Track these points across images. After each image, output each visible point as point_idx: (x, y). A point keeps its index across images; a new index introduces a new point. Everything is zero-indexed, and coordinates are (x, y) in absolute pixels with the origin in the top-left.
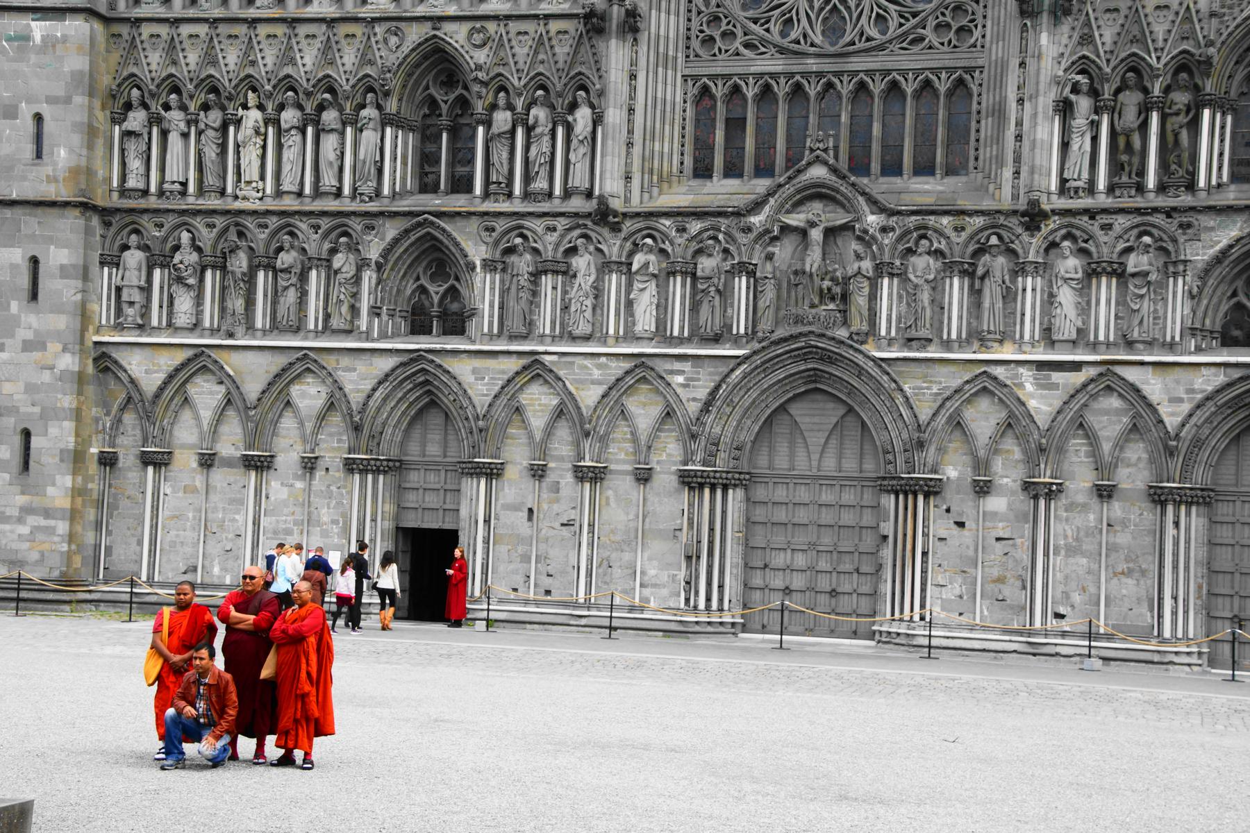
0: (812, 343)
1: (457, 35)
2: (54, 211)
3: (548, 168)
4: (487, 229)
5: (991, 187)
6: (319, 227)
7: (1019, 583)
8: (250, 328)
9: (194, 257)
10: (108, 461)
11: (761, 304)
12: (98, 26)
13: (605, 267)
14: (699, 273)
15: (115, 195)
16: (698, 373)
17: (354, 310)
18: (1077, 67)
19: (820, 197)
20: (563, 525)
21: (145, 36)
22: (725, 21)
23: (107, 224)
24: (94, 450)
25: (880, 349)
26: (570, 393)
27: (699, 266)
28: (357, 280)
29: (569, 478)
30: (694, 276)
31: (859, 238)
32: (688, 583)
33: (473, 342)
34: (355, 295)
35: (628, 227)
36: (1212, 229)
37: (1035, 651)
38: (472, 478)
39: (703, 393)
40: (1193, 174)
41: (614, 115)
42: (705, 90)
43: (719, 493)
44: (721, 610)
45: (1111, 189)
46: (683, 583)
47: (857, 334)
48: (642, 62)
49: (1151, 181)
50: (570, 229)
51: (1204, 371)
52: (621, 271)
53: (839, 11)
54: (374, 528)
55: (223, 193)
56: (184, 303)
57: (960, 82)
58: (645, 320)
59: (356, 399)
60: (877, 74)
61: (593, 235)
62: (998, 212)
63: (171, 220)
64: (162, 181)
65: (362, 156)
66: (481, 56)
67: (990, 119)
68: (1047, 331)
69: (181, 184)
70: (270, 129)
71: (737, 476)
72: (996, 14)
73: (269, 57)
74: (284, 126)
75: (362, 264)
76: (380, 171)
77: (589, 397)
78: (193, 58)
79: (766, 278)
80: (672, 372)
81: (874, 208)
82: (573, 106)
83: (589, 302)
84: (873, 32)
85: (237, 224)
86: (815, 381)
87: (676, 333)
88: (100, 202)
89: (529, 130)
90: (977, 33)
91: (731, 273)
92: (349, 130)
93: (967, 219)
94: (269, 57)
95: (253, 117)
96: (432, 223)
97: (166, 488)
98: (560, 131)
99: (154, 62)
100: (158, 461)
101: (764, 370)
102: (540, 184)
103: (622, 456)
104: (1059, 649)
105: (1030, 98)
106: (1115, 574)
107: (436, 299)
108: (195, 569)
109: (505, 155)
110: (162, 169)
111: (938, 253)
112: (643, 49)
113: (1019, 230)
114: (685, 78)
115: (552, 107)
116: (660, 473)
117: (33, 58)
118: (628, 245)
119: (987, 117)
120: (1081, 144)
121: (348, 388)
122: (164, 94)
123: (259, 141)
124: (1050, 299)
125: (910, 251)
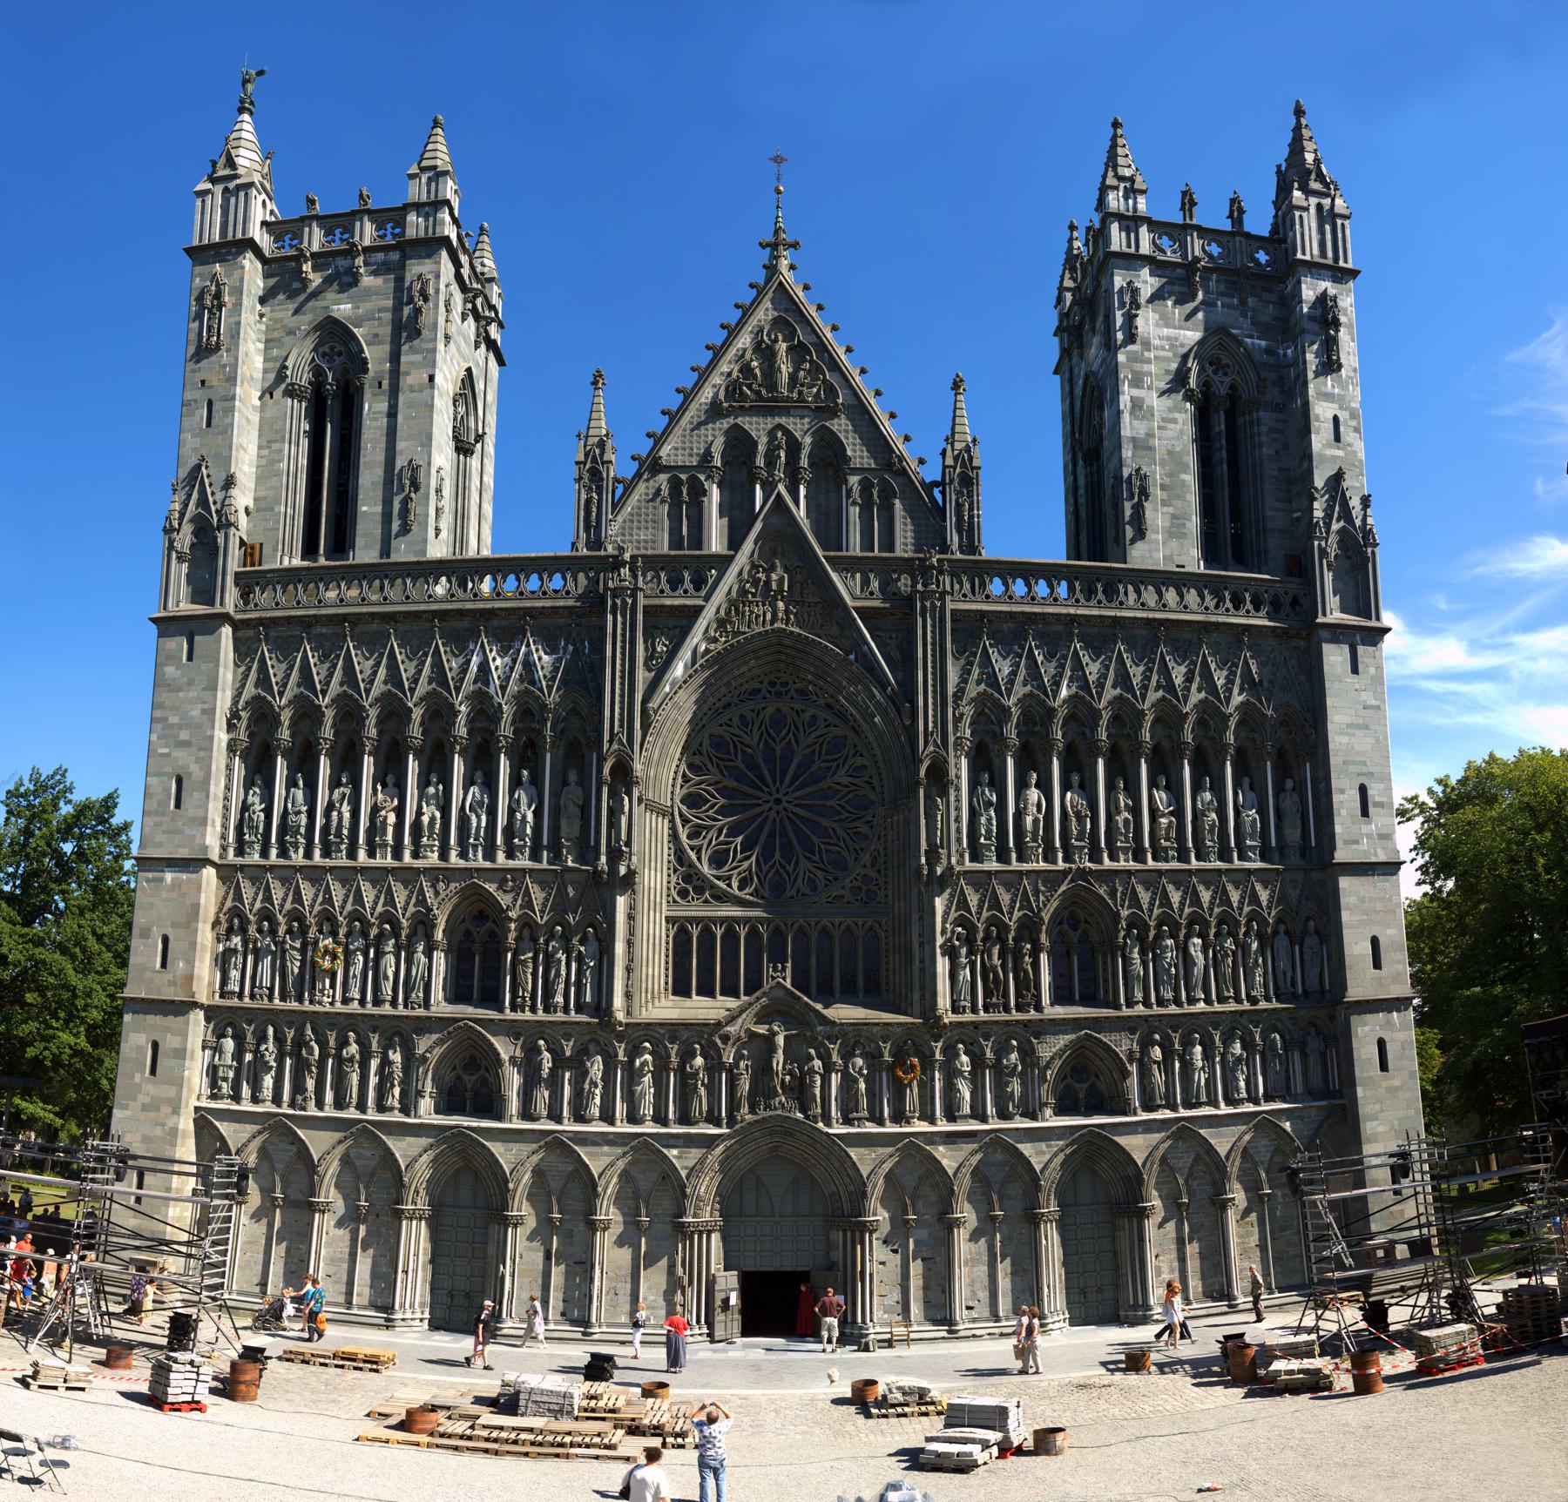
7: (940, 1289)
40: (1038, 997)
49: (1012, 1003)
57: (871, 929)
61: (601, 1039)
64: (253, 986)
84: (807, 890)
90: (881, 894)
102: (559, 999)
114: (668, 919)
117: (164, 894)
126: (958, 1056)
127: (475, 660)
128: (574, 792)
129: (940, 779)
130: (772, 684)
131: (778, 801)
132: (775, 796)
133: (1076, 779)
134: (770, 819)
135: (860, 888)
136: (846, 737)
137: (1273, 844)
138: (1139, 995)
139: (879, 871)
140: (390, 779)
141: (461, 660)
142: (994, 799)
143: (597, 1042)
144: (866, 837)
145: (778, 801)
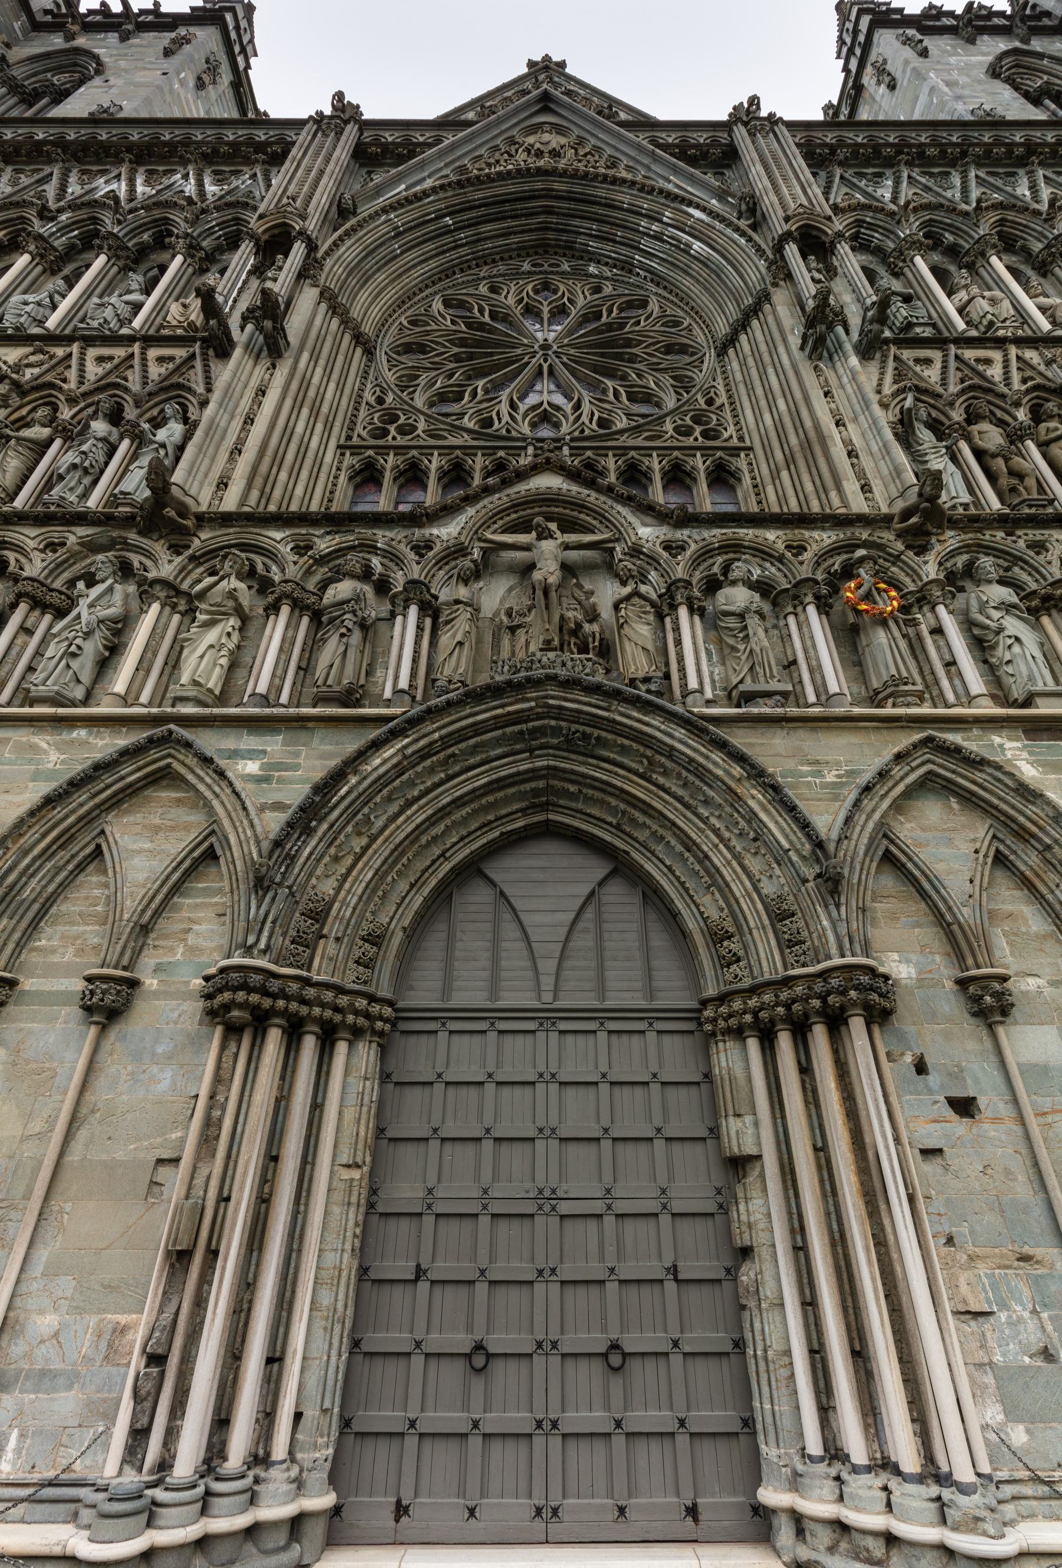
0: (551, 702)
3: (87, 481)
11: (446, 640)
16: (297, 755)
22: (403, 418)
43: (309, 1044)
46: (136, 1362)
47: (647, 680)
50: (91, 547)
52: (174, 606)
60: (610, 453)
61: (135, 559)
62: (862, 520)
67: (785, 474)
71: (361, 1003)
72: (759, 391)
79: (457, 602)
80: (235, 754)
81: (648, 520)
82: (158, 423)
83: (92, 648)
86: (544, 807)
93: (807, 534)
98: (125, 445)
101: (445, 763)
105: (855, 419)
111: (763, 588)
113: (900, 546)
116: (156, 994)
119: (775, 475)
125: (713, 586)
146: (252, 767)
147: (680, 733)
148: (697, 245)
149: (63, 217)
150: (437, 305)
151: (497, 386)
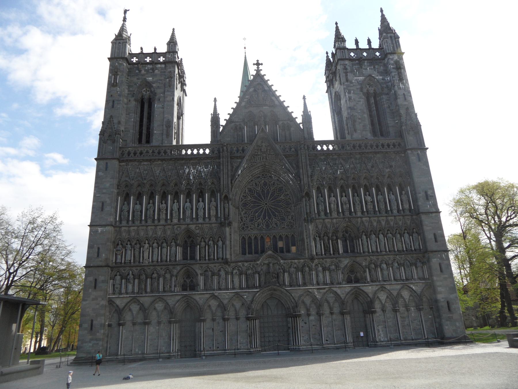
1: (193, 227)
2: (99, 268)
4: (201, 267)
5: (303, 255)
6: (162, 268)
8: (146, 292)
9: (132, 276)
10: (110, 325)
11: (261, 280)
12: (113, 228)
13: (227, 273)
14: (248, 274)
15: (114, 264)
17: (170, 287)
18: (316, 232)
19: (270, 257)
20: (220, 332)
21: (122, 230)
23: (112, 271)
24: (107, 323)
25: (286, 287)
26: (222, 301)
27: (248, 273)
28: (171, 279)
29: (221, 320)
30: (246, 274)
31: (279, 265)
32: (250, 342)
33: (198, 291)
34: (171, 283)
35: (232, 265)
36: (344, 261)
37: (324, 348)
38: (199, 322)
39: (250, 299)
40: (338, 251)
41: (228, 243)
42: (243, 238)
44: (257, 347)
45: (325, 254)
48: (232, 232)
49: (332, 253)
51: (347, 288)
53: (268, 222)
54: (176, 336)
55: (139, 262)
56: (130, 287)
57: (293, 235)
58: (237, 284)
59: (171, 306)
61: (224, 267)
63: (128, 268)
65: (172, 252)
66: (198, 231)
67: (300, 242)
68: (317, 282)
69: (129, 260)
70: (151, 248)
73: (150, 233)
74: (154, 247)
75: (172, 276)
76: (176, 256)
77: (225, 302)
78: (133, 234)
80: (243, 295)
83: (224, 281)
84: (275, 226)
85: (143, 269)
87: (244, 287)
88: (110, 265)
89: (208, 246)
90: (295, 226)
91: (254, 273)
92: (169, 247)
94: (150, 233)
95: (147, 246)
96: (189, 266)
97: (124, 331)
99: (125, 235)
100: (123, 325)
102: (212, 257)
103: (233, 315)
104: (330, 348)
106: (336, 330)
107: (188, 283)
108: (132, 351)
109: (204, 251)
110: (125, 258)
112: (232, 229)
113: (310, 262)
115: (214, 241)
118: (232, 269)
119: (299, 241)
120: (318, 246)
121: (170, 304)
122: (126, 242)
123: (148, 250)
124: (317, 276)
126: (319, 267)
127: (187, 171)
128: (213, 203)
129: (308, 195)
130: (263, 175)
131: (266, 204)
132: (266, 203)
133: (344, 194)
134: (264, 209)
135: (289, 225)
136: (282, 187)
137: (401, 209)
138: (366, 250)
139: (294, 221)
140: (164, 202)
141: (183, 171)
142: (323, 201)
143: (223, 268)
144: (289, 212)
145: (266, 204)
146: (245, 297)
147: (285, 291)
148: (291, 182)
149: (184, 183)
150: (247, 190)
151: (259, 216)
